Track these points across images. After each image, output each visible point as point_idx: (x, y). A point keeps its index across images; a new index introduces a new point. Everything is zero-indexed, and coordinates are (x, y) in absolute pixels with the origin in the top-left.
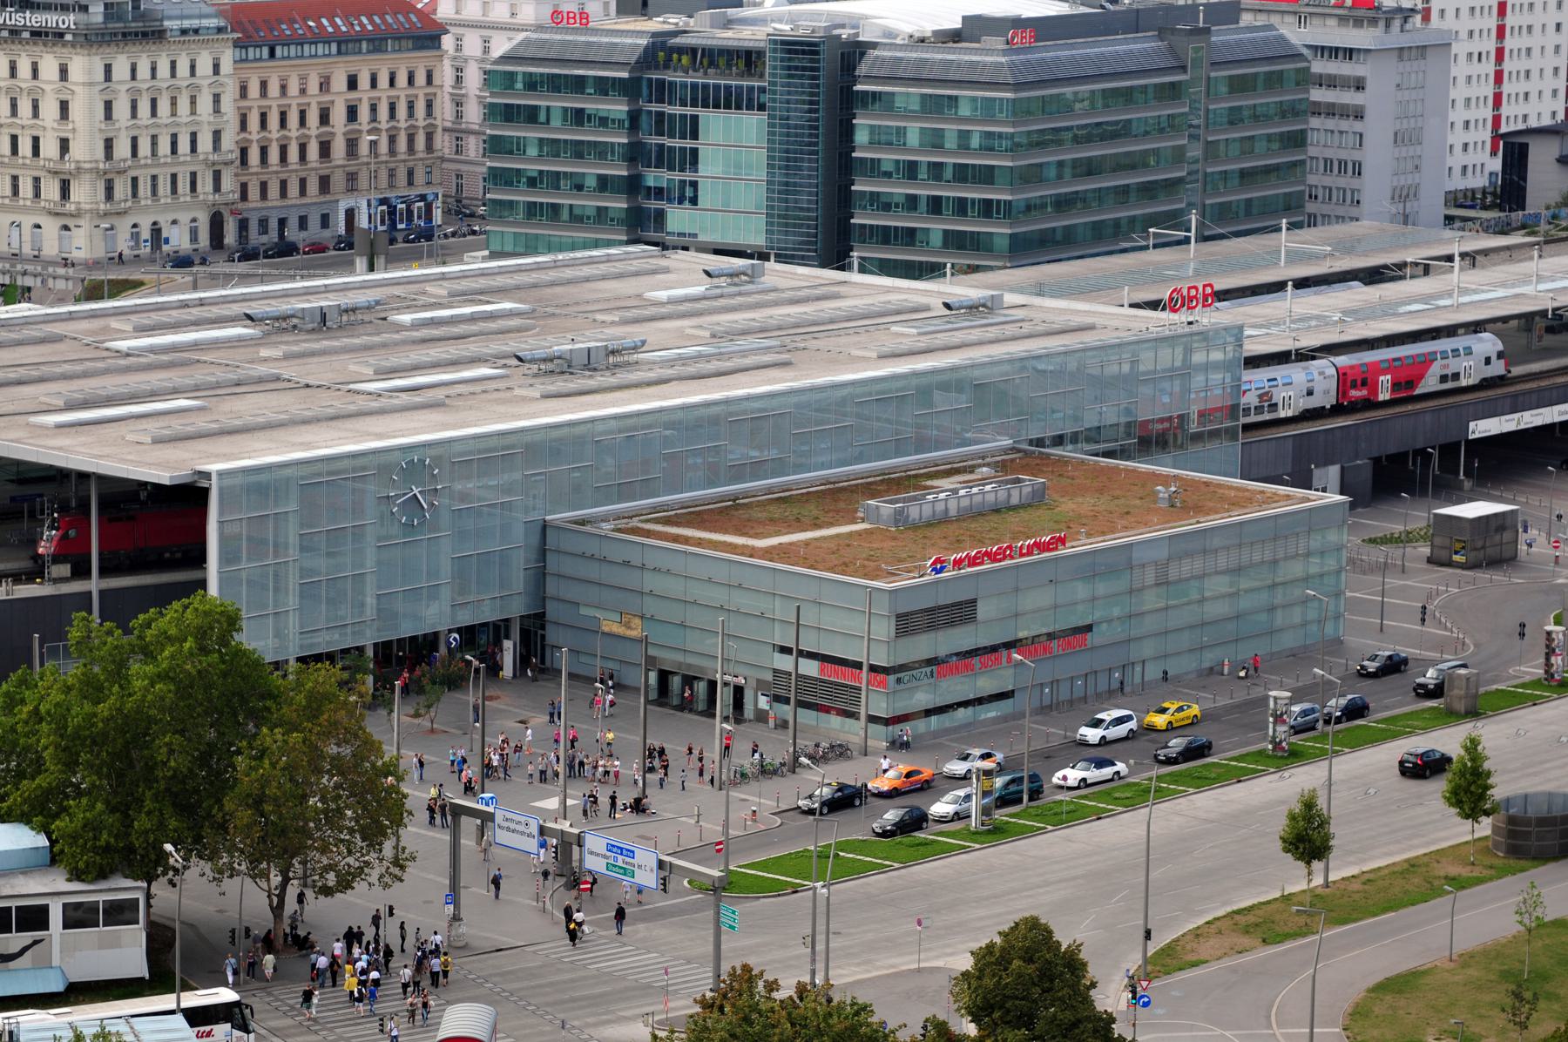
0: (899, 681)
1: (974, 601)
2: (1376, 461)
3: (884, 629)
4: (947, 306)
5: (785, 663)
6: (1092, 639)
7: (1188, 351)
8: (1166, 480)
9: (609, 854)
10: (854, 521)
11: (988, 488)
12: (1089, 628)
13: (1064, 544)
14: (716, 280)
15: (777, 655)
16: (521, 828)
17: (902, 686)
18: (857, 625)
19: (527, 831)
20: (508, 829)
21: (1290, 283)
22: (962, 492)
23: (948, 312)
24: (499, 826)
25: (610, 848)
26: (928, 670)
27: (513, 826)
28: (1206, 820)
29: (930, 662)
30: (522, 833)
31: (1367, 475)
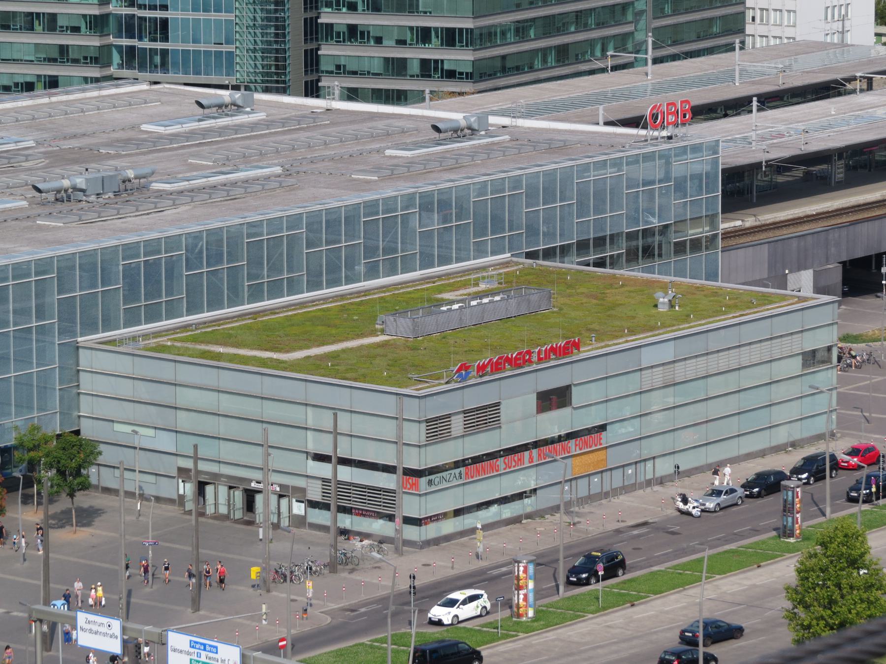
0: (430, 483)
1: (498, 404)
2: (844, 263)
3: (415, 433)
4: (436, 129)
5: (325, 470)
6: (607, 438)
7: (668, 163)
8: (664, 287)
9: (192, 650)
10: (373, 333)
11: (497, 298)
12: (603, 428)
13: (578, 349)
14: (207, 111)
15: (311, 463)
16: (101, 629)
17: (433, 488)
18: (388, 430)
19: (110, 632)
20: (91, 631)
21: (755, 99)
22: (474, 303)
23: (436, 135)
24: (82, 629)
25: (193, 645)
26: (457, 471)
27: (95, 628)
28: (734, 604)
29: (457, 464)
30: (105, 634)
31: (837, 277)
